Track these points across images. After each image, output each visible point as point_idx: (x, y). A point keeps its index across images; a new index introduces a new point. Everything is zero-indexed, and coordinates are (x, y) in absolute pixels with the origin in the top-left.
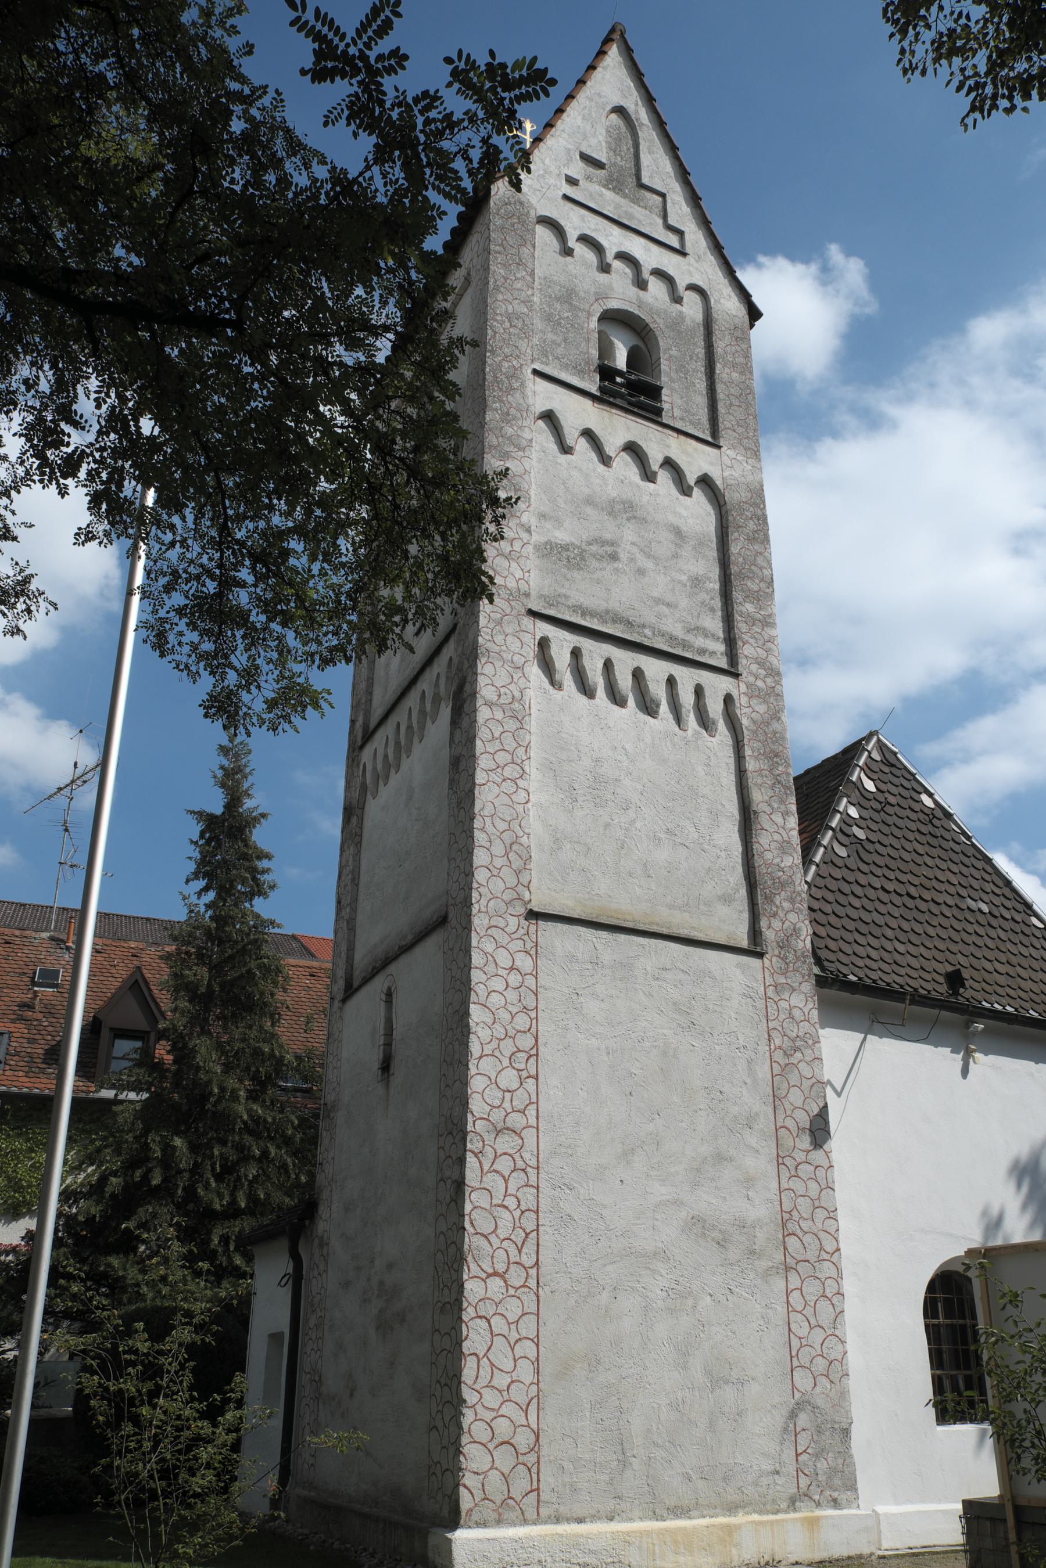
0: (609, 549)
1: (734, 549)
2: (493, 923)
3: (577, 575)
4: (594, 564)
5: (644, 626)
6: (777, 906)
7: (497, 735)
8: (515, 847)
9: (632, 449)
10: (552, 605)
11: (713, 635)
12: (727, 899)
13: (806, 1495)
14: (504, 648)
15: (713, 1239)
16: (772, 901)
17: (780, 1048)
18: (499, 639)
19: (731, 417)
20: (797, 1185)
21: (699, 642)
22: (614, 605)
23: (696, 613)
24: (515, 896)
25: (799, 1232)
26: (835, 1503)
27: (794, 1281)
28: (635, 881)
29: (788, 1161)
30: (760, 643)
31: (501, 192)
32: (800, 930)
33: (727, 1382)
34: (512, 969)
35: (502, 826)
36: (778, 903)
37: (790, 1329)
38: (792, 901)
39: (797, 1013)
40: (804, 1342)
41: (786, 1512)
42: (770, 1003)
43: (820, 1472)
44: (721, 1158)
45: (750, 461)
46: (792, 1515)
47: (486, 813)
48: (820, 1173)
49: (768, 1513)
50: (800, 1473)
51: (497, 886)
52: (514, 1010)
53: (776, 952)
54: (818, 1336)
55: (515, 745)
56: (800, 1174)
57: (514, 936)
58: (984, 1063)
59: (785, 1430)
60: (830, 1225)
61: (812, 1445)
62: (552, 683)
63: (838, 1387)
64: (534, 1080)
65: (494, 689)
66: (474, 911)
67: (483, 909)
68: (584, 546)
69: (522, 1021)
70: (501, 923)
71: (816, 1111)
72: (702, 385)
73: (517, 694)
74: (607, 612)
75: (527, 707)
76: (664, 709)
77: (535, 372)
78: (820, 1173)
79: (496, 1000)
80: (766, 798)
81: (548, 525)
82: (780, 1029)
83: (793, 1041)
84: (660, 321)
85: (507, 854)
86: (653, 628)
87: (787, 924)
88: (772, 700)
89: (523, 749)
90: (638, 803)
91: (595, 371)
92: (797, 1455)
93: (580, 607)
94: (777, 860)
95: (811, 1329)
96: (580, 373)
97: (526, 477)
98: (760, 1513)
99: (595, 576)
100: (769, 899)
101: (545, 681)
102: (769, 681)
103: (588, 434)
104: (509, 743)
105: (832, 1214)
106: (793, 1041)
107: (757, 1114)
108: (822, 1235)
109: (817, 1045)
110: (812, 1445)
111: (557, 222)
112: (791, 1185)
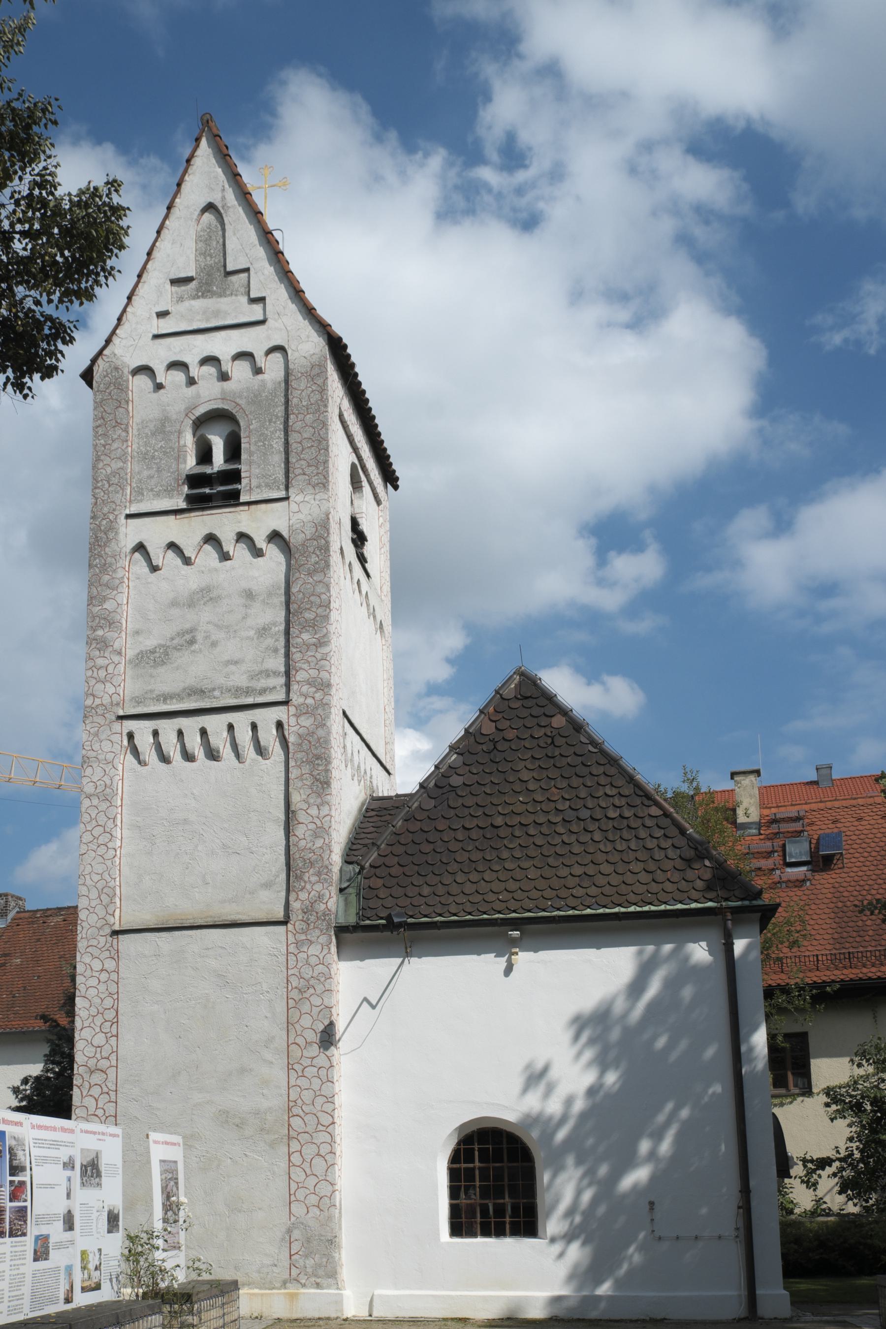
0: (188, 637)
1: (294, 589)
2: (89, 944)
3: (161, 670)
4: (176, 654)
5: (214, 689)
6: (305, 882)
7: (93, 817)
8: (105, 891)
9: (211, 539)
10: (141, 702)
11: (274, 673)
12: (268, 885)
13: (296, 1280)
14: (100, 752)
15: (234, 1124)
16: (301, 878)
17: (296, 988)
18: (96, 747)
19: (303, 462)
20: (303, 1082)
21: (263, 683)
22: (191, 681)
23: (260, 660)
24: (105, 922)
25: (302, 1114)
26: (318, 1286)
27: (294, 1145)
28: (196, 889)
29: (296, 1067)
30: (312, 664)
31: (101, 367)
32: (323, 895)
33: (240, 1211)
34: (102, 970)
35: (96, 878)
36: (306, 879)
37: (290, 1178)
38: (319, 874)
39: (313, 960)
40: (300, 1185)
41: (279, 1289)
42: (292, 958)
43: (308, 1266)
44: (243, 1071)
45: (317, 497)
46: (283, 1291)
47: (86, 872)
48: (323, 1072)
49: (266, 1289)
50: (292, 1266)
51: (93, 919)
52: (103, 996)
53: (300, 917)
54: (312, 1181)
55: (106, 819)
56: (305, 1074)
57: (102, 949)
58: (524, 959)
59: (283, 1239)
60: (328, 1107)
61: (303, 1249)
62: (140, 762)
63: (326, 1213)
64: (116, 1038)
65: (93, 784)
66: (79, 939)
67: (84, 936)
68: (168, 643)
69: (108, 1002)
70: (94, 942)
71: (321, 1027)
72: (278, 445)
73: (108, 782)
74: (184, 689)
75: (115, 789)
76: (227, 752)
77: (129, 516)
78: (323, 1072)
79: (92, 992)
80: (304, 797)
81: (141, 639)
82: (298, 974)
83: (308, 981)
84: (242, 402)
85: (99, 896)
86: (220, 688)
87: (313, 893)
88: (320, 711)
89: (112, 820)
90: (202, 832)
91: (183, 483)
92: (291, 1256)
93: (163, 695)
94: (309, 845)
95: (307, 1176)
96: (168, 492)
97: (119, 610)
98: (261, 1288)
99: (175, 665)
100: (299, 878)
101: (135, 762)
102: (318, 696)
103: (172, 546)
104: (102, 819)
105: (330, 1100)
106: (308, 981)
107: (273, 1038)
108: (320, 1114)
109: (328, 981)
110: (303, 1249)
111: (147, 366)
112: (299, 1082)
